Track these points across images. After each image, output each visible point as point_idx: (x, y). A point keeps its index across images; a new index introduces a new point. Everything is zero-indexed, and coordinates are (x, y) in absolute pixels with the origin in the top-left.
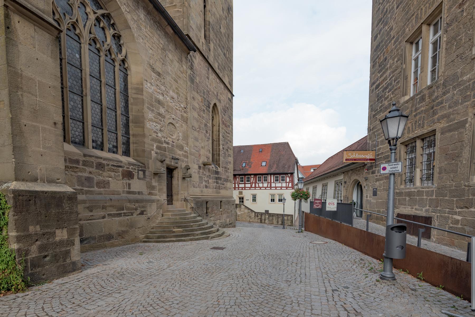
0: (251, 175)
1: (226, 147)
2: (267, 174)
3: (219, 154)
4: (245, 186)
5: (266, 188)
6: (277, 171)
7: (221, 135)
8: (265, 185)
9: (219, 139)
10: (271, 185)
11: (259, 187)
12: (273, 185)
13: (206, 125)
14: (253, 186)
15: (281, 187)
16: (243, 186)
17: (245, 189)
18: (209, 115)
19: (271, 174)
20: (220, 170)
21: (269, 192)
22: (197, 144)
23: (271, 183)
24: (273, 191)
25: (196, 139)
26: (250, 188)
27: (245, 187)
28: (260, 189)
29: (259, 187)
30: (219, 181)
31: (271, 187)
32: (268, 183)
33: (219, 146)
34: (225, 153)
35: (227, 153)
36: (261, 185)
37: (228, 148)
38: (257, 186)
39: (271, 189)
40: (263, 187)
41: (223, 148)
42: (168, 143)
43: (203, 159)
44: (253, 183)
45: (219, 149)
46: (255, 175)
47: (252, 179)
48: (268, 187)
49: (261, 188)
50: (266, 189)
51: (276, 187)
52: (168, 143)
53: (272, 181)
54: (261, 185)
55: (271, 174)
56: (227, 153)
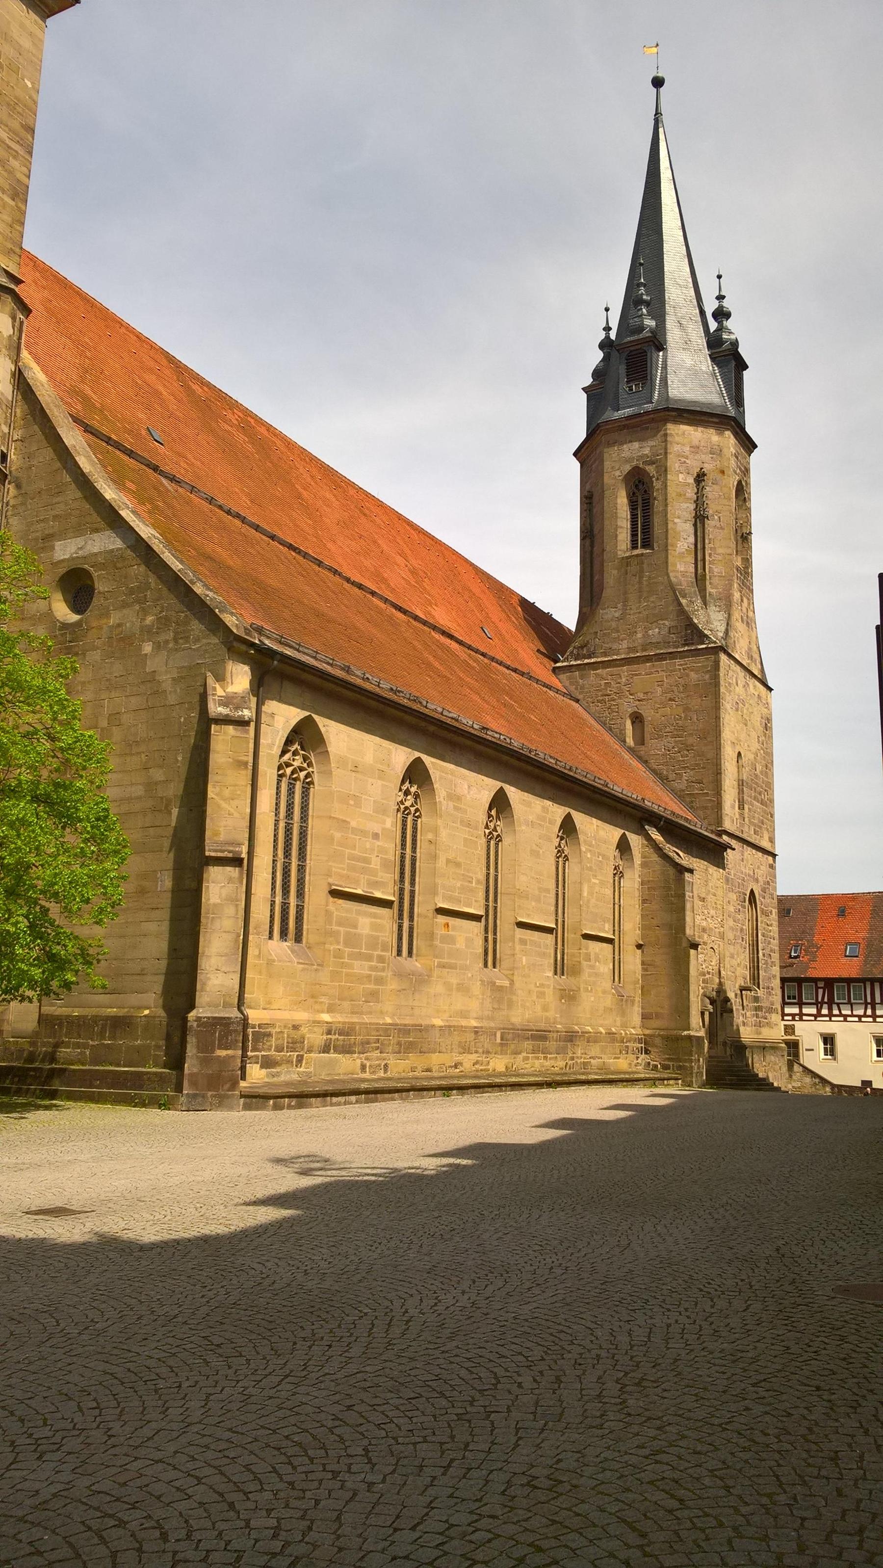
0: (815, 980)
1: (767, 952)
2: (863, 981)
3: (758, 966)
4: (801, 1010)
5: (860, 1017)
7: (759, 934)
9: (757, 941)
11: (841, 1015)
13: (742, 930)
14: (825, 1011)
16: (796, 1010)
17: (801, 1020)
18: (744, 912)
20: (760, 993)
22: (734, 962)
25: (732, 957)
26: (816, 1016)
27: (801, 1015)
28: (845, 1020)
30: (760, 1013)
33: (758, 953)
34: (766, 963)
35: (769, 960)
37: (771, 951)
39: (875, 1021)
40: (852, 1016)
41: (764, 955)
42: (709, 973)
43: (740, 982)
44: (823, 1003)
45: (758, 957)
46: (829, 983)
47: (820, 991)
48: (865, 1016)
49: (845, 1016)
50: (860, 1021)
52: (709, 973)
56: (769, 960)
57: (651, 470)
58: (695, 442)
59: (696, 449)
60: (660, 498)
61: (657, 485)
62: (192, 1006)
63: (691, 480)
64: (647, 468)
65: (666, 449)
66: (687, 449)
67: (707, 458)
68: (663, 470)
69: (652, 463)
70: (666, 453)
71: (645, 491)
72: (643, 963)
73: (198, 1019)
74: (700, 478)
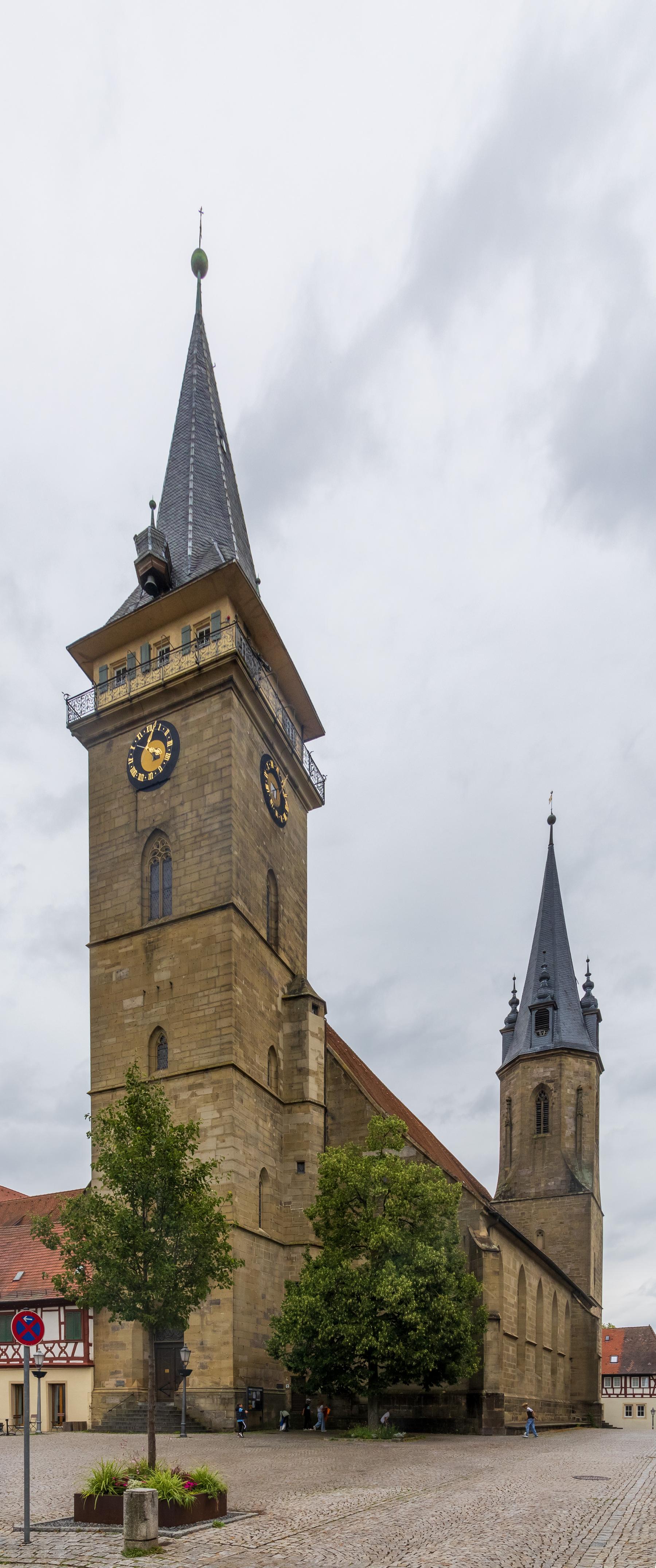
2: (621, 1376)
5: (618, 1395)
6: (636, 1372)
8: (617, 1391)
10: (626, 1391)
11: (607, 1394)
12: (629, 1391)
15: (642, 1395)
19: (626, 1376)
21: (622, 1402)
23: (626, 1388)
24: (630, 1401)
29: (607, 1394)
31: (626, 1394)
32: (622, 1388)
36: (610, 1391)
38: (604, 1392)
49: (609, 1395)
51: (634, 1395)
53: (628, 1385)
54: (610, 1391)
55: (626, 1376)
57: (551, 1085)
58: (576, 1069)
59: (577, 1073)
60: (556, 1103)
61: (555, 1095)
62: (482, 1388)
63: (574, 1093)
64: (549, 1084)
65: (561, 1073)
66: (572, 1073)
67: (582, 1079)
68: (559, 1087)
69: (552, 1081)
70: (561, 1076)
71: (546, 1099)
72: (572, 1368)
73: (487, 1394)
74: (579, 1090)
